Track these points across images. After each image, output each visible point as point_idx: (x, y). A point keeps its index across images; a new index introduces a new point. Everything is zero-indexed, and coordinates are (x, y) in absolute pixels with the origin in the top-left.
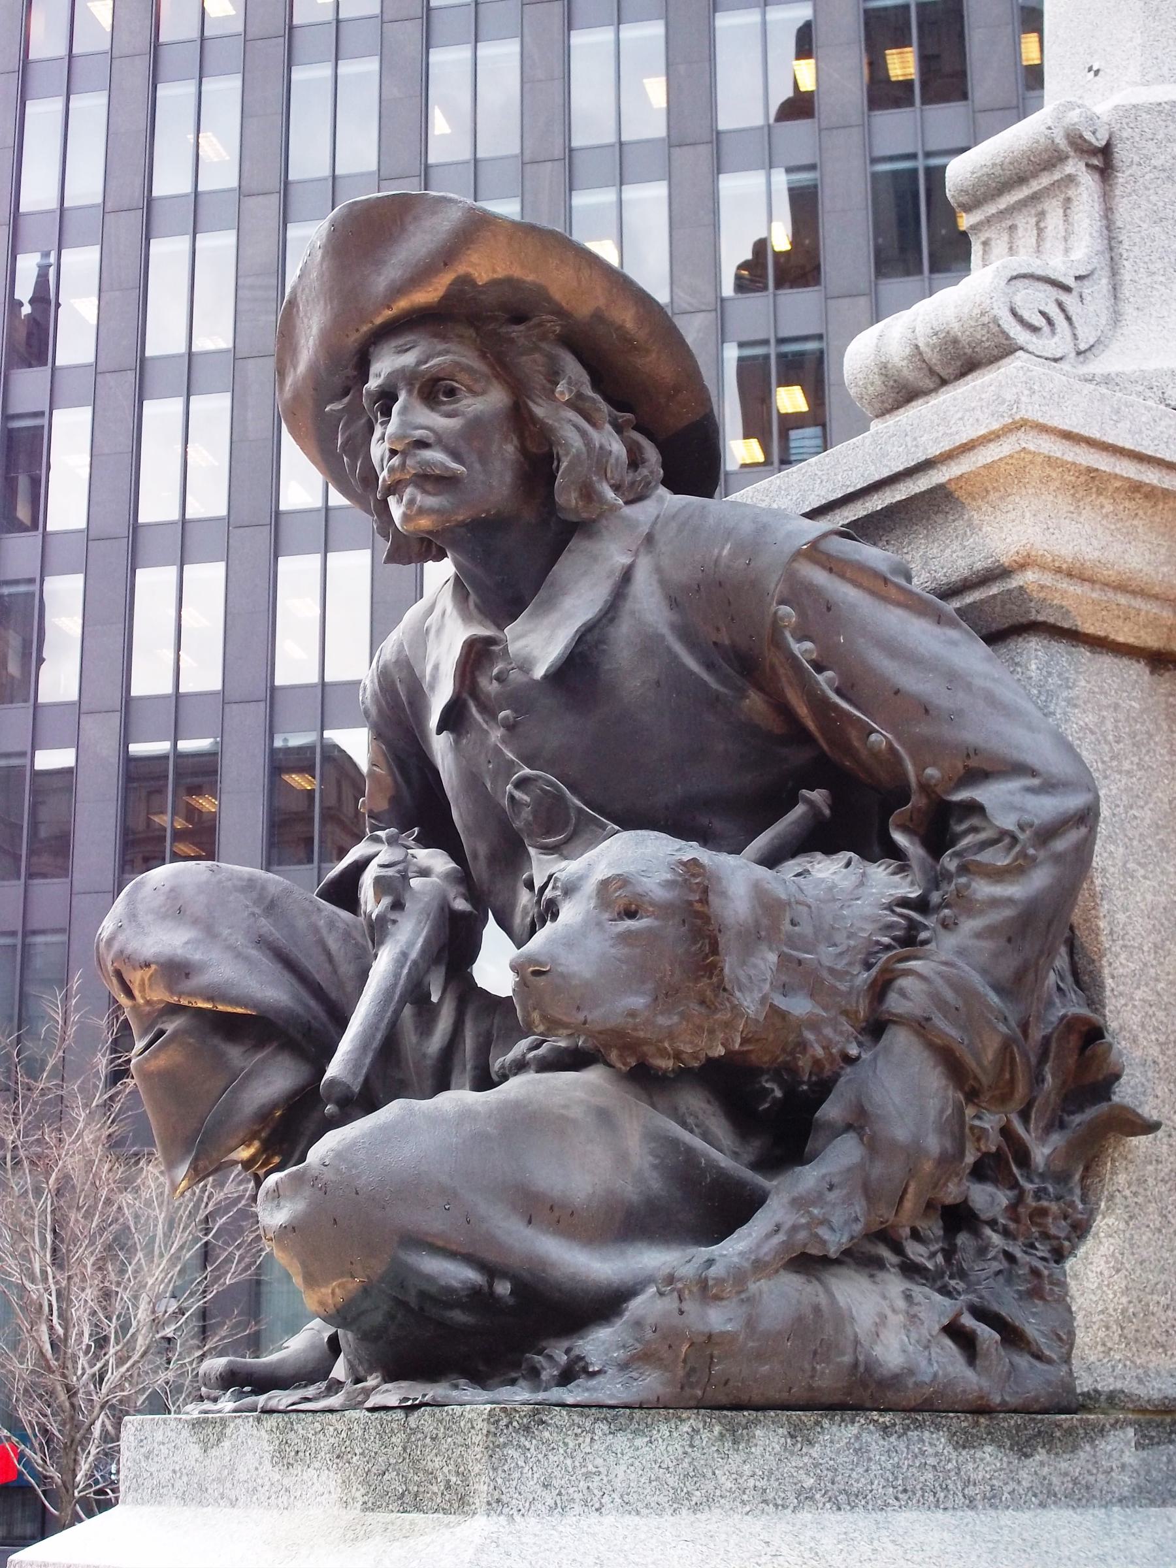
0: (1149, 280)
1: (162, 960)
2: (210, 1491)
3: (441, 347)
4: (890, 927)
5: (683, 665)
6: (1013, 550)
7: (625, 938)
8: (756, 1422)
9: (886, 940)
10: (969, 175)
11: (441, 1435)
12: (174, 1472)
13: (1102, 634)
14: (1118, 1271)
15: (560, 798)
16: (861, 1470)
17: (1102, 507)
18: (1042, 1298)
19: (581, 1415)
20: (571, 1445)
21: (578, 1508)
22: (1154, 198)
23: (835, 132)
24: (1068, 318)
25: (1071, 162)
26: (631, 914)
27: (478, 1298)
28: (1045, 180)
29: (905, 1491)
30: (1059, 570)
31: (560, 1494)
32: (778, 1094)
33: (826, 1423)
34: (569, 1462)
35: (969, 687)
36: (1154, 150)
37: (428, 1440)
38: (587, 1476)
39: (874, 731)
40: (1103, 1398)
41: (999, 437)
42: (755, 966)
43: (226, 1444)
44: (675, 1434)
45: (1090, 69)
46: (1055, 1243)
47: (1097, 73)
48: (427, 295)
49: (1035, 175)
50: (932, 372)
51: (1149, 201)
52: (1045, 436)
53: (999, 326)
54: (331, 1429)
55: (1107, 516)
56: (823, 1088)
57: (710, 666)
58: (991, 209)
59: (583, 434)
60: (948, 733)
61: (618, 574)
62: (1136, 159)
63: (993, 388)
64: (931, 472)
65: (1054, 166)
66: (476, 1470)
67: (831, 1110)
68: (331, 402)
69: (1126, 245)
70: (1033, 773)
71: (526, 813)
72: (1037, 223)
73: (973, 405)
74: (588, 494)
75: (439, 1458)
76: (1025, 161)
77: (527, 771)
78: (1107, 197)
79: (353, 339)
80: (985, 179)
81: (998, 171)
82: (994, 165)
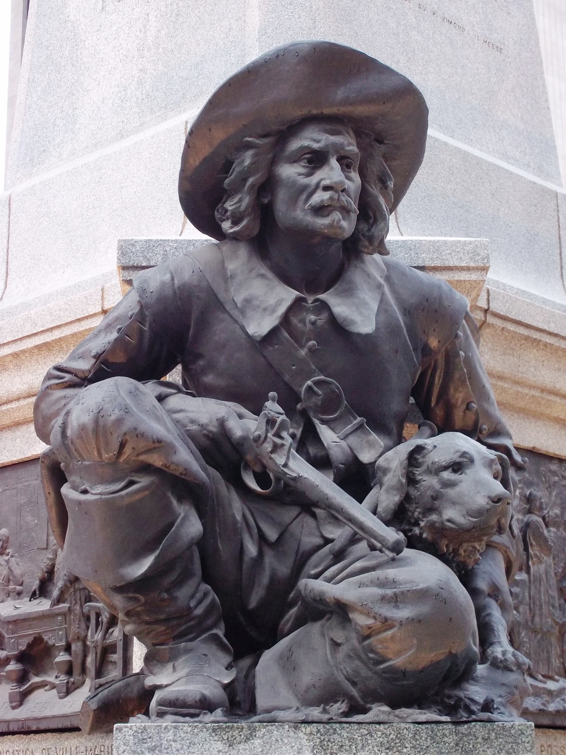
15: (339, 396)
37: (480, 740)
41: (469, 270)
43: (257, 742)
68: (250, 136)
73: (458, 250)
75: (490, 750)
77: (322, 377)
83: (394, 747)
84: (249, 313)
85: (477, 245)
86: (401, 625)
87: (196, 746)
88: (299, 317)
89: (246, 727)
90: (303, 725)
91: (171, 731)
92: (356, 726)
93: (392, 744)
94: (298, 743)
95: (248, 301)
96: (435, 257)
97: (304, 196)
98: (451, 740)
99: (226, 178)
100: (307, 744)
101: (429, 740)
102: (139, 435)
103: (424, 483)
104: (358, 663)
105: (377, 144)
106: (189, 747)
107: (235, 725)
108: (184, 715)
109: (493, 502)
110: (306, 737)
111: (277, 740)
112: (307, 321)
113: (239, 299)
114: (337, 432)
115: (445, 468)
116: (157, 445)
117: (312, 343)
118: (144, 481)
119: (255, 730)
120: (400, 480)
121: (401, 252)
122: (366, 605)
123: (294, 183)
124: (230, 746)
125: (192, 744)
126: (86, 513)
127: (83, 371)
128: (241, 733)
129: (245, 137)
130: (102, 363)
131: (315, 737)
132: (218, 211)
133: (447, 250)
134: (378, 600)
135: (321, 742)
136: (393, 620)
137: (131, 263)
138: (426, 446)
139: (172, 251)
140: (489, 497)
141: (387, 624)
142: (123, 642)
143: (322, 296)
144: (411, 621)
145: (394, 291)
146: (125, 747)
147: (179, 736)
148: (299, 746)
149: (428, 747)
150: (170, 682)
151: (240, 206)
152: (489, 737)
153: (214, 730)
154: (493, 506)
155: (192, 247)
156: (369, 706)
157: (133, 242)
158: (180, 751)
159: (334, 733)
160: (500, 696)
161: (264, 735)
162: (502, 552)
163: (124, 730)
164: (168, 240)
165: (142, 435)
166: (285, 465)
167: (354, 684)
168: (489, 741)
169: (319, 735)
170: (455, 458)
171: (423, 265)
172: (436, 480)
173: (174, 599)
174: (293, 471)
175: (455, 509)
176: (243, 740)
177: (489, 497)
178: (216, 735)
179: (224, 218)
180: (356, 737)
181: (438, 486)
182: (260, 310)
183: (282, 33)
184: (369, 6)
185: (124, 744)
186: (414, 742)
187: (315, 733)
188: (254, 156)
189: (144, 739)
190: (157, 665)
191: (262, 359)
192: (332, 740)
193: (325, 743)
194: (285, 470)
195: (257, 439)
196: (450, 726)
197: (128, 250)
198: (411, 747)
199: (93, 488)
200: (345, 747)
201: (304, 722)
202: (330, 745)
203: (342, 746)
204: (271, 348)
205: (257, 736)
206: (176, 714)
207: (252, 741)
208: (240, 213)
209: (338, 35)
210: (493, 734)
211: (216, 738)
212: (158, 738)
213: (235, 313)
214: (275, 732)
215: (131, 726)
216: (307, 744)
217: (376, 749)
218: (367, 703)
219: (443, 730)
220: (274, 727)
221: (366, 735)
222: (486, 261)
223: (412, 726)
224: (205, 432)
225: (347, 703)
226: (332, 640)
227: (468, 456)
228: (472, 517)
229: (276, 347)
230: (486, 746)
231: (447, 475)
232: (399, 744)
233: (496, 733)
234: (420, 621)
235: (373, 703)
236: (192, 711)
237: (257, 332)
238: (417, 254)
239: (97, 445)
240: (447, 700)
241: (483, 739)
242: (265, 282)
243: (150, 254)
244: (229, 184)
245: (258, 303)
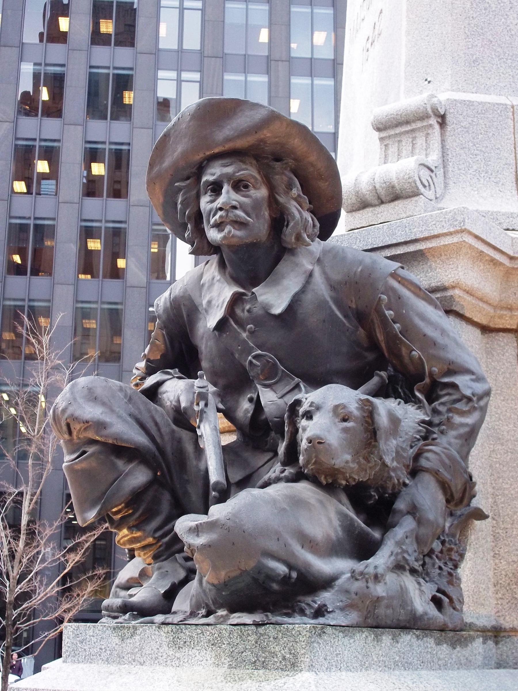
0: (459, 172)
1: (95, 420)
2: (126, 658)
3: (244, 166)
4: (419, 431)
5: (336, 315)
6: (451, 280)
7: (345, 430)
8: (383, 633)
9: (418, 437)
10: (384, 117)
11: (280, 637)
12: (101, 649)
13: (471, 317)
14: (472, 574)
15: (275, 365)
16: (411, 653)
17: (480, 266)
18: (452, 585)
19: (335, 629)
20: (332, 642)
21: (334, 669)
22: (461, 139)
23: (75, 51)
24: (434, 184)
25: (432, 119)
26: (344, 420)
27: (286, 579)
28: (419, 124)
29: (423, 662)
30: (465, 291)
31: (329, 663)
32: (377, 497)
33: (402, 634)
34: (332, 649)
35: (448, 336)
36: (462, 119)
37: (271, 639)
38: (337, 655)
39: (413, 350)
40: (468, 625)
41: (452, 234)
42: (389, 445)
43: (137, 638)
44: (361, 638)
45: (426, 80)
46: (454, 562)
47: (429, 82)
48: (240, 144)
49: (414, 121)
50: (379, 198)
51: (459, 140)
52: (470, 236)
53: (416, 184)
54: (208, 633)
55: (481, 270)
56: (395, 496)
57: (346, 316)
58: (392, 132)
59: (300, 213)
60: (442, 354)
61: (308, 273)
62: (455, 122)
63: (451, 214)
64: (416, 244)
65: (424, 119)
66: (302, 652)
67: (401, 505)
68: (178, 182)
69: (450, 156)
70: (473, 373)
71: (258, 370)
72: (412, 141)
73: (441, 219)
74: (299, 237)
75: (278, 647)
76: (412, 115)
77: (259, 352)
78: (442, 135)
79: (198, 157)
81: (399, 117)
82: (397, 115)
84: (210, 311)
85: (455, 212)
92: (194, 627)
93: (216, 641)
94: (160, 639)
95: (209, 302)
96: (423, 229)
98: (252, 638)
102: (76, 419)
105: (275, 163)
106: (100, 641)
110: (165, 635)
111: (148, 637)
118: (91, 450)
121: (399, 230)
133: (433, 221)
145: (324, 273)
146: (68, 640)
149: (237, 644)
152: (277, 637)
159: (181, 632)
160: (342, 601)
161: (141, 633)
162: (434, 476)
163: (69, 627)
165: (76, 418)
171: (415, 238)
180: (194, 635)
183: (421, 60)
184: (506, 15)
186: (229, 640)
189: (78, 634)
192: (180, 638)
201: (163, 624)
203: (185, 642)
204: (225, 335)
206: (109, 616)
209: (469, 48)
210: (281, 635)
211: (115, 635)
214: (147, 631)
216: (165, 640)
217: (206, 644)
219: (247, 630)
220: (147, 627)
222: (462, 224)
223: (228, 627)
224: (172, 406)
232: (220, 642)
233: (282, 634)
234: (210, 546)
236: (116, 614)
238: (410, 229)
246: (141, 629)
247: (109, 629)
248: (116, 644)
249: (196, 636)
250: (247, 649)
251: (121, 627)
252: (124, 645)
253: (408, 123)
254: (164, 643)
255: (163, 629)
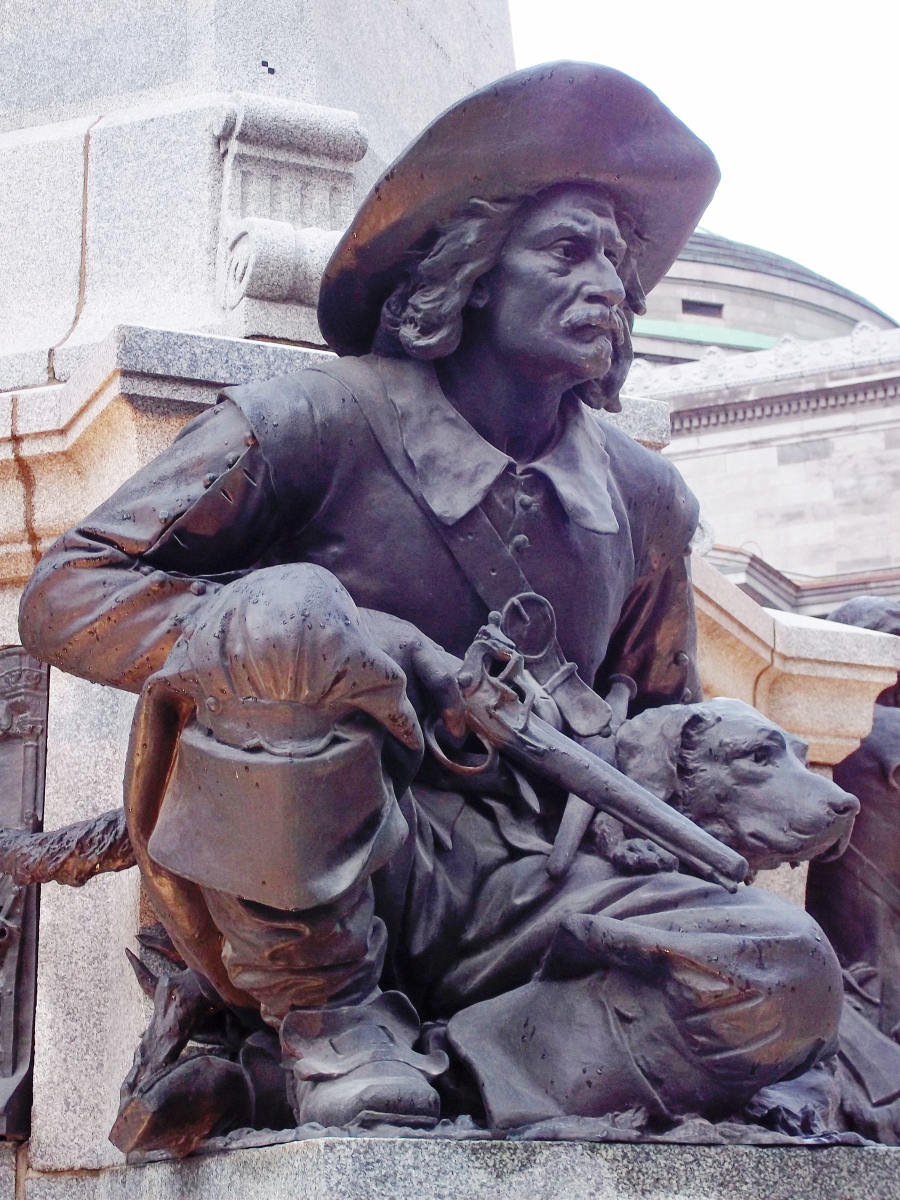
37: (845, 1173)
43: (538, 1170)
45: (265, 64)
49: (318, 154)
68: (481, 198)
80: (283, 131)
81: (298, 133)
82: (296, 127)
83: (729, 1182)
84: (434, 479)
86: (770, 994)
87: (448, 1177)
88: (504, 495)
89: (521, 1147)
90: (603, 1146)
91: (410, 1152)
93: (728, 1178)
94: (596, 1174)
95: (430, 459)
97: (555, 307)
98: (807, 1172)
99: (423, 258)
100: (609, 1175)
101: (777, 1172)
103: (701, 774)
104: (667, 1049)
107: (505, 1143)
108: (415, 1126)
109: (836, 811)
110: (607, 1165)
111: (566, 1169)
112: (517, 503)
113: (417, 453)
114: (542, 681)
115: (744, 754)
116: (389, 682)
117: (521, 538)
118: (354, 739)
119: (534, 1153)
120: (667, 767)
122: (716, 960)
123: (542, 283)
124: (498, 1176)
125: (442, 1172)
126: (257, 784)
127: (137, 543)
128: (514, 1157)
129: (473, 197)
130: (177, 532)
131: (620, 1164)
132: (388, 307)
134: (734, 954)
135: (628, 1172)
136: (757, 984)
137: (138, 367)
138: (704, 717)
139: (204, 356)
140: (831, 805)
141: (747, 991)
142: (15, 997)
143: (538, 464)
144: (781, 986)
146: (340, 1177)
147: (422, 1159)
148: (598, 1179)
149: (776, 1183)
150: (344, 1071)
151: (441, 305)
152: (856, 1169)
153: (474, 1151)
154: (837, 817)
155: (236, 354)
156: (677, 1117)
157: (143, 332)
158: (424, 1184)
159: (647, 1160)
161: (547, 1160)
163: (338, 1148)
164: (199, 337)
166: (525, 730)
167: (656, 1082)
168: (857, 1176)
169: (625, 1162)
170: (761, 739)
172: (727, 771)
173: (346, 934)
174: (538, 740)
175: (763, 818)
176: (517, 1168)
177: (831, 805)
178: (477, 1158)
179: (399, 320)
180: (677, 1165)
181: (730, 781)
182: (450, 476)
185: (339, 1171)
186: (757, 1175)
187: (620, 1159)
188: (483, 229)
189: (368, 1164)
190: (299, 1041)
191: (445, 557)
192: (644, 1170)
193: (635, 1174)
194: (524, 737)
195: (465, 685)
196: (805, 1151)
197: (134, 344)
198: (754, 1183)
199: (276, 743)
200: (662, 1182)
202: (642, 1177)
203: (658, 1179)
204: (462, 539)
205: (538, 1161)
206: (398, 1124)
207: (530, 1170)
208: (439, 318)
210: (862, 1165)
211: (477, 1164)
212: (390, 1163)
213: (405, 474)
214: (563, 1156)
215: (349, 1142)
216: (609, 1175)
217: (705, 1184)
218: (673, 1112)
219: (795, 1157)
220: (561, 1149)
221: (691, 1163)
223: (753, 1150)
225: (645, 1112)
226: (617, 1012)
227: (779, 738)
228: (800, 832)
229: (470, 538)
230: (853, 1183)
231: (746, 765)
232: (736, 1178)
233: (866, 1164)
235: (682, 1114)
236: (422, 1119)
237: (447, 512)
239: (296, 673)
240: (746, 1109)
241: (849, 1171)
242: (458, 432)
243: (170, 356)
244: (428, 268)
245: (446, 464)
246: (546, 1153)
247: (460, 1150)
248: (482, 1185)
249: (683, 1167)
250: (796, 1193)
251: (494, 1146)
252: (503, 1187)
253: (304, 150)
254: (605, 1182)
255: (604, 1153)
